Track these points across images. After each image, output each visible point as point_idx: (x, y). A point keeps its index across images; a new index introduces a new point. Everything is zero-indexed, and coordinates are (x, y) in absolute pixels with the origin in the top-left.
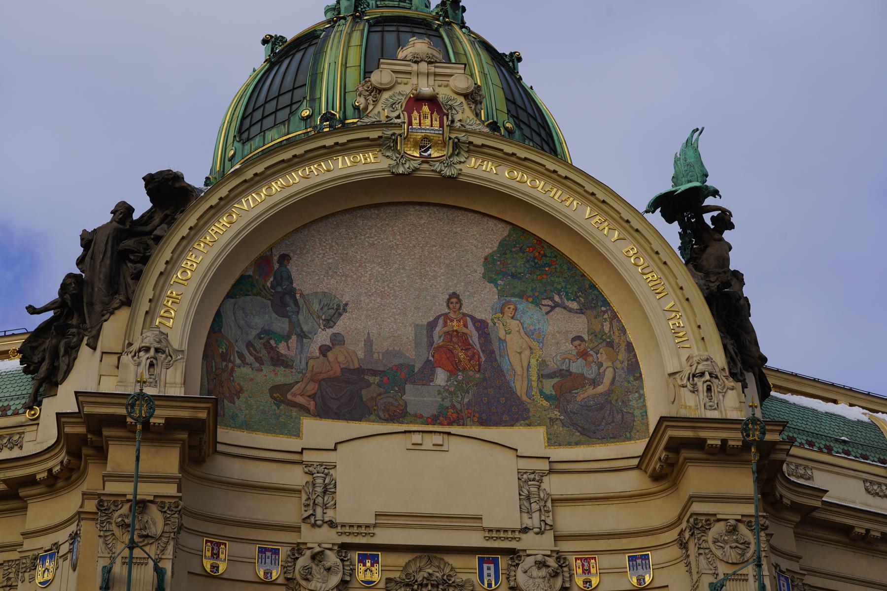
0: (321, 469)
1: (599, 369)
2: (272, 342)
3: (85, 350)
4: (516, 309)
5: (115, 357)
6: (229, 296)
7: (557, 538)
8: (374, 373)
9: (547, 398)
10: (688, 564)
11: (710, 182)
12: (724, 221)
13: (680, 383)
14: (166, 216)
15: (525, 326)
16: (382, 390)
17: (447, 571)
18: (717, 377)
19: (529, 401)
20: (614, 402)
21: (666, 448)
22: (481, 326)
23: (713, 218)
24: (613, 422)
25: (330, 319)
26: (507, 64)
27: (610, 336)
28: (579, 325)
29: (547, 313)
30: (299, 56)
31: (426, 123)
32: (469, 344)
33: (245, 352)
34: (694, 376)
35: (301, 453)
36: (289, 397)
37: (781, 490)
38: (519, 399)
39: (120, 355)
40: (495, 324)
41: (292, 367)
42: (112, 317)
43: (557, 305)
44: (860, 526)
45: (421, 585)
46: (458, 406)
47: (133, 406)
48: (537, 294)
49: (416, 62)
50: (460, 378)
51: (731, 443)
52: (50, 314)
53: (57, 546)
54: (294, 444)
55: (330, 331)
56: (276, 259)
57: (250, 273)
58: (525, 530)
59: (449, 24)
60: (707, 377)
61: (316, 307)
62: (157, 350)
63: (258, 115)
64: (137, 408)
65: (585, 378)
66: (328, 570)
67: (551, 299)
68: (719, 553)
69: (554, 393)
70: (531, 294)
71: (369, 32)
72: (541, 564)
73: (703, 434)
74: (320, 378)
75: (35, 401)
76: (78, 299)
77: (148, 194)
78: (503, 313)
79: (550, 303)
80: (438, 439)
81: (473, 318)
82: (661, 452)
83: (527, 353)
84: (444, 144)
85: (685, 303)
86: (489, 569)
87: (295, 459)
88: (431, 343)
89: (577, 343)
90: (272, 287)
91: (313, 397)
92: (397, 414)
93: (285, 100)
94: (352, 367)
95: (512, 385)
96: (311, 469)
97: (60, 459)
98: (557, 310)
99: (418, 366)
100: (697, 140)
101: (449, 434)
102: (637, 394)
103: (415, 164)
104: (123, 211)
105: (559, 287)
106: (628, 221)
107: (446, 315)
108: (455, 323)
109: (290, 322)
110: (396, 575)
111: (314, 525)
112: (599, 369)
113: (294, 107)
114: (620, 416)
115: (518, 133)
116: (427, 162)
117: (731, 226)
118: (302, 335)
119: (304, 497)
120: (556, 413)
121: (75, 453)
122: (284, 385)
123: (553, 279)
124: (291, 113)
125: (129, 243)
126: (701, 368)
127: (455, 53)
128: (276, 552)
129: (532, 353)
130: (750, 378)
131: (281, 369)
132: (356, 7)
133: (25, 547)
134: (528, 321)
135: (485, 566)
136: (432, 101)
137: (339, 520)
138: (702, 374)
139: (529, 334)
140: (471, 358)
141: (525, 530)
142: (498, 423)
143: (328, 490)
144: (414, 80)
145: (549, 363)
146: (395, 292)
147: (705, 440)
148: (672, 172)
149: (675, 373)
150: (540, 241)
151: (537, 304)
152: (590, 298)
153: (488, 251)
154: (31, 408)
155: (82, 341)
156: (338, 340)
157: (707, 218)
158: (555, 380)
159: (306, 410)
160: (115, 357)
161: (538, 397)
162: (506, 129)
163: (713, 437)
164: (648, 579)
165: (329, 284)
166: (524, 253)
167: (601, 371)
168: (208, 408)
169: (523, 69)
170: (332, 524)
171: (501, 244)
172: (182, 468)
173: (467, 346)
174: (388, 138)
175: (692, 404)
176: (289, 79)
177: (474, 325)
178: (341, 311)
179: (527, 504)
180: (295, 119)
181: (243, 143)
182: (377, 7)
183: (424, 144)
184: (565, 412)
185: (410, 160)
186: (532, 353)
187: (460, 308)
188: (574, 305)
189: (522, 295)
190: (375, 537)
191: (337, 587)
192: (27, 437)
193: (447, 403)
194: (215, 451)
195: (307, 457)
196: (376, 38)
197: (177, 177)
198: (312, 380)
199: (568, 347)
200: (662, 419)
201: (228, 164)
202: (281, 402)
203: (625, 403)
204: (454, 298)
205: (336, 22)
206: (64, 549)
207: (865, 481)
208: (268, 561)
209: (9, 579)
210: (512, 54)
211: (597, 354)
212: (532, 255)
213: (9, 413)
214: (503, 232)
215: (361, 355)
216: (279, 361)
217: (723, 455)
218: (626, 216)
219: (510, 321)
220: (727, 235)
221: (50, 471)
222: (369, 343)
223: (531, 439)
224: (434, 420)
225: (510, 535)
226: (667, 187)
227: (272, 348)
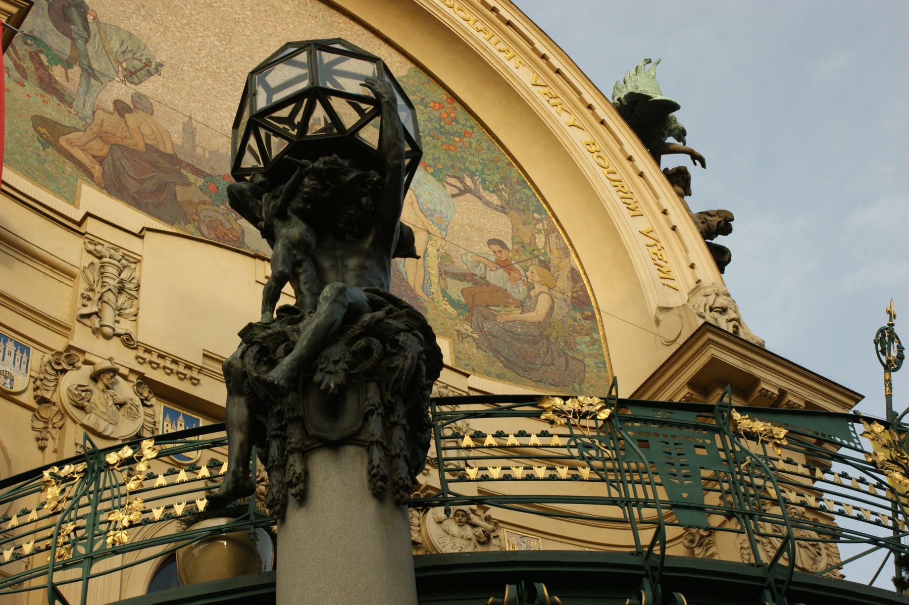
1: (529, 290)
2: (43, 58)
8: (198, 172)
9: (454, 304)
16: (206, 198)
19: (427, 299)
20: (552, 339)
21: (691, 384)
24: (553, 364)
25: (135, 73)
27: (545, 254)
28: (501, 226)
29: (454, 196)
36: (62, 141)
38: (412, 291)
48: (440, 166)
61: (115, 45)
65: (509, 296)
67: (462, 181)
69: (463, 300)
70: (431, 163)
74: (113, 140)
79: (459, 184)
89: (497, 248)
91: (101, 160)
94: (162, 148)
95: (402, 269)
98: (468, 195)
102: (587, 339)
105: (473, 168)
109: (73, 46)
112: (529, 290)
114: (562, 360)
120: (466, 327)
122: (56, 123)
123: (465, 156)
128: (25, 349)
129: (430, 239)
131: (54, 101)
145: (456, 260)
146: (235, 80)
152: (518, 196)
158: (465, 285)
161: (439, 297)
165: (137, 25)
166: (426, 107)
167: (532, 293)
170: (128, 341)
178: (152, 69)
184: (481, 330)
186: (430, 239)
188: (494, 199)
190: (199, 387)
198: (100, 137)
202: (50, 143)
203: (570, 346)
211: (525, 271)
212: (437, 114)
215: (177, 139)
222: (189, 130)
227: (42, 64)
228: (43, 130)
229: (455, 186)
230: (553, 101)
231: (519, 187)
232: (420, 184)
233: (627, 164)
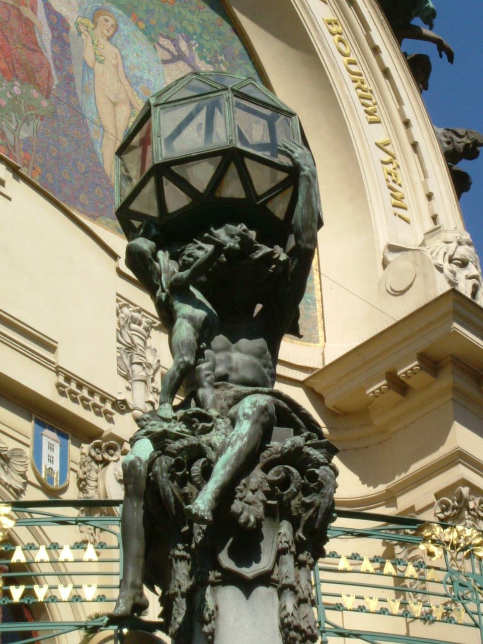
4: (116, 28)
15: (128, 63)
22: (59, 24)
29: (165, 62)
32: (36, 44)
40: (80, 33)
48: (153, 22)
67: (176, 44)
79: (172, 48)
86: (51, 448)
95: (99, 150)
105: (190, 29)
123: (183, 12)
134: (132, 59)
177: (48, 17)
219: (103, 42)
229: (168, 50)
231: (241, 62)
232: (128, 42)
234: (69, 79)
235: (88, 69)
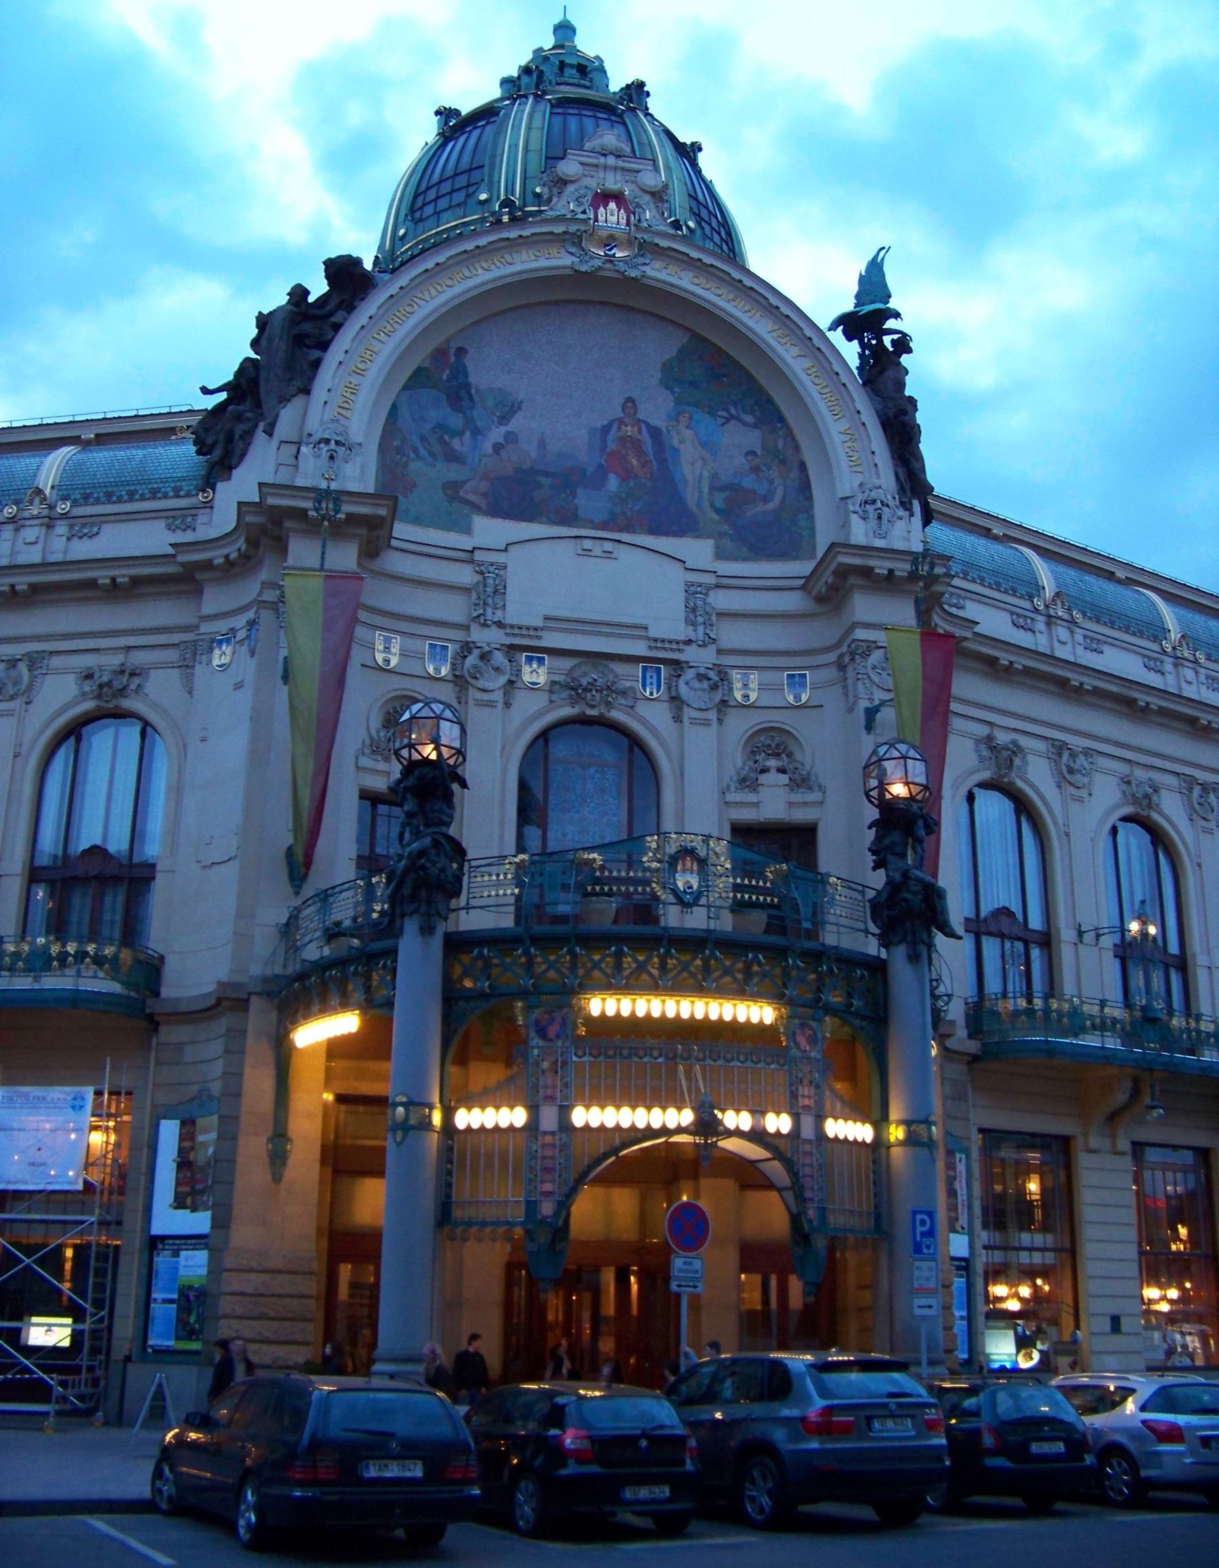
0: (491, 569)
2: (446, 437)
3: (260, 436)
4: (691, 418)
5: (294, 448)
6: (405, 388)
7: (720, 652)
8: (547, 474)
9: (717, 511)
10: (845, 687)
11: (893, 304)
12: (903, 345)
13: (852, 508)
14: (342, 302)
17: (611, 677)
18: (887, 506)
21: (835, 573)
22: (655, 433)
23: (893, 341)
26: (688, 153)
28: (753, 439)
30: (477, 132)
31: (611, 217)
33: (419, 445)
34: (866, 502)
35: (472, 552)
36: (462, 494)
37: (936, 619)
39: (299, 444)
41: (464, 463)
42: (289, 405)
43: (733, 417)
44: (1004, 658)
45: (586, 690)
46: (629, 514)
47: (320, 503)
49: (604, 155)
50: (632, 484)
51: (898, 573)
52: (223, 396)
53: (233, 631)
54: (466, 542)
55: (503, 429)
56: (453, 351)
57: (426, 365)
58: (689, 642)
59: (633, 110)
60: (879, 505)
61: (490, 403)
62: (337, 443)
63: (432, 195)
64: (324, 505)
66: (497, 669)
67: (729, 412)
68: (876, 678)
71: (551, 113)
72: (701, 677)
73: (872, 563)
75: (209, 482)
76: (254, 383)
77: (327, 277)
78: (678, 422)
79: (726, 415)
80: (608, 546)
81: (647, 425)
82: (827, 576)
83: (700, 463)
84: (629, 243)
85: (862, 428)
87: (468, 556)
88: (603, 448)
89: (750, 457)
90: (448, 380)
91: (484, 495)
92: (567, 517)
93: (462, 181)
96: (483, 568)
97: (237, 546)
98: (733, 422)
99: (591, 470)
100: (883, 259)
101: (619, 541)
103: (598, 263)
104: (299, 293)
106: (810, 339)
107: (621, 421)
108: (629, 428)
110: (561, 678)
111: (485, 625)
113: (471, 190)
115: (699, 232)
116: (611, 262)
117: (909, 351)
118: (476, 432)
119: (474, 595)
121: (253, 543)
124: (468, 196)
125: (307, 327)
126: (873, 495)
127: (640, 143)
130: (916, 505)
131: (454, 466)
132: (537, 87)
133: (203, 629)
135: (648, 675)
136: (618, 198)
137: (508, 621)
138: (874, 502)
139: (704, 444)
140: (644, 465)
141: (689, 642)
142: (667, 534)
143: (500, 591)
144: (601, 174)
147: (872, 568)
148: (855, 288)
149: (847, 498)
150: (719, 350)
151: (712, 413)
153: (666, 357)
154: (204, 491)
155: (256, 426)
156: (511, 438)
157: (887, 340)
159: (477, 508)
160: (294, 448)
162: (688, 227)
163: (881, 566)
164: (804, 698)
168: (387, 506)
169: (702, 159)
170: (500, 625)
171: (680, 351)
172: (359, 564)
173: (640, 453)
174: (574, 234)
175: (860, 533)
176: (466, 159)
177: (649, 433)
179: (692, 617)
180: (472, 201)
181: (416, 223)
182: (558, 84)
183: (610, 242)
185: (592, 258)
187: (635, 413)
188: (749, 419)
189: (697, 405)
191: (504, 686)
192: (202, 518)
193: (618, 510)
194: (389, 546)
195: (479, 556)
196: (558, 120)
197: (357, 262)
199: (740, 461)
200: (833, 545)
201: (398, 243)
204: (630, 403)
205: (515, 100)
206: (241, 635)
207: (1012, 613)
208: (438, 657)
209: (185, 659)
210: (693, 144)
213: (182, 493)
214: (681, 339)
215: (534, 454)
216: (453, 457)
217: (888, 583)
218: (808, 333)
220: (905, 359)
221: (227, 557)
222: (542, 444)
223: (698, 551)
224: (604, 526)
225: (674, 646)
226: (849, 306)
227: (446, 443)
228: (449, 492)
230: (784, 341)
233: (835, 377)
234: (663, 462)
235: (676, 450)
